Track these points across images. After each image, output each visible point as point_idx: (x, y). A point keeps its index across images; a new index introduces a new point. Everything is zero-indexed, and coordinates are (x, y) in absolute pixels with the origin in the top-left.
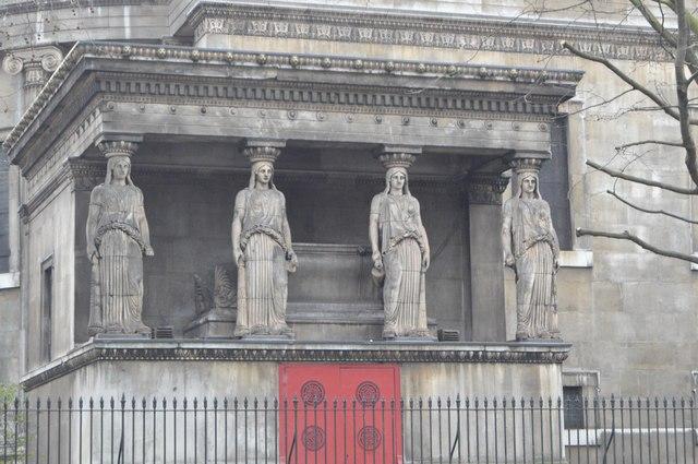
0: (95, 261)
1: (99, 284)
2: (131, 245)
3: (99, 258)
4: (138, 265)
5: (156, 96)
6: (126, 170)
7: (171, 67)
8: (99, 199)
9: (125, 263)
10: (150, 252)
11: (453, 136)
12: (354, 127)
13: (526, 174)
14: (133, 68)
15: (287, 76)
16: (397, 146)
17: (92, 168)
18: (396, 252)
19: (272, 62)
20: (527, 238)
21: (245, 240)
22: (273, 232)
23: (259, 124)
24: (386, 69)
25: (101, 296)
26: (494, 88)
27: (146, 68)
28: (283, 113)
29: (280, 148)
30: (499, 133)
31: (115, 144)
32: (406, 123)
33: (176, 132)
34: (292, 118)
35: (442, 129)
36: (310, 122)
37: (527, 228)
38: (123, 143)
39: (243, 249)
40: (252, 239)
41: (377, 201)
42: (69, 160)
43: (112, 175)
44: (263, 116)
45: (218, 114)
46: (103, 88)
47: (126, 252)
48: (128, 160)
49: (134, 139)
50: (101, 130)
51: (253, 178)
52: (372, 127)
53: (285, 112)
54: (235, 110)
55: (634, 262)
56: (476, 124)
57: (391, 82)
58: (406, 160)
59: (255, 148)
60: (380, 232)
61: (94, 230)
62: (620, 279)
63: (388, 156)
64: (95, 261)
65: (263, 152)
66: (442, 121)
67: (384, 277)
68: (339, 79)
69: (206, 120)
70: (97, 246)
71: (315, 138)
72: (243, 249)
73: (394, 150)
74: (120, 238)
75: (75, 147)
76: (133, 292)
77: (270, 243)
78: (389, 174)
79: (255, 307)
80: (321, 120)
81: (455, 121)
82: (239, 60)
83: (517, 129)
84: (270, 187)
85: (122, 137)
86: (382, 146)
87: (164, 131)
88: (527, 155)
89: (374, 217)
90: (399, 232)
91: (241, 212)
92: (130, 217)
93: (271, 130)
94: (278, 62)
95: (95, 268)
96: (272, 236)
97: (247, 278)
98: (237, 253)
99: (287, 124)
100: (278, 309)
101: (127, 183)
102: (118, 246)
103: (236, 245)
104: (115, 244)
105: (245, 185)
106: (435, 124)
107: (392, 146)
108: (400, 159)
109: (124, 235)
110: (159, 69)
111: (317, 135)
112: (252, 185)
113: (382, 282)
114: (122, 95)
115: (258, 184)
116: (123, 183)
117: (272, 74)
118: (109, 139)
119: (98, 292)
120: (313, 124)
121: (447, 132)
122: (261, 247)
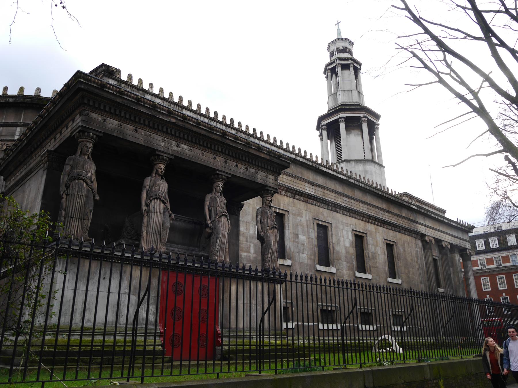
0: (64, 196)
1: (65, 210)
2: (88, 190)
3: (67, 195)
4: (92, 202)
5: (114, 115)
6: (90, 150)
7: (124, 101)
8: (71, 163)
9: (83, 200)
10: (98, 198)
11: (243, 173)
12: (204, 158)
13: (268, 197)
14: (105, 95)
15: (180, 123)
16: (222, 171)
17: (70, 146)
18: (219, 221)
19: (175, 114)
20: (269, 225)
21: (149, 201)
22: (164, 200)
23: (162, 144)
24: (223, 133)
25: (65, 218)
26: (262, 155)
27: (112, 97)
28: (174, 143)
29: (169, 159)
30: (261, 177)
31: (86, 134)
32: (226, 162)
33: (121, 137)
34: (178, 146)
35: (240, 169)
36: (185, 149)
37: (269, 220)
38: (91, 134)
39: (147, 205)
40: (153, 201)
41: (208, 197)
42: (48, 151)
43: (81, 152)
44: (164, 141)
45: (143, 133)
46: (86, 101)
47: (85, 193)
48: (92, 145)
49: (98, 134)
50: (80, 124)
51: (155, 172)
52: (212, 160)
53: (174, 142)
54: (152, 134)
55: (250, 256)
56: (253, 171)
57: (224, 140)
58: (224, 179)
59: (159, 155)
60: (210, 211)
61: (66, 178)
62: (245, 262)
63: (216, 176)
64: (64, 196)
65: (163, 159)
66: (240, 166)
67: (212, 233)
68: (203, 132)
69: (137, 135)
70: (67, 187)
71: (187, 158)
72: (147, 205)
73: (220, 173)
74: (82, 185)
75: (52, 145)
76: (86, 218)
77: (162, 205)
78: (215, 185)
79: (152, 237)
80: (190, 150)
81: (244, 167)
82: (160, 108)
83: (266, 176)
84: (162, 178)
85: (91, 131)
86: (216, 170)
87: (115, 134)
88: (270, 189)
89: (207, 204)
90: (221, 213)
91: (147, 187)
92: (89, 175)
93: (168, 149)
94: (177, 115)
95: (64, 200)
96: (163, 202)
97: (148, 222)
98: (144, 208)
99: (175, 148)
100: (163, 241)
101: (89, 158)
102: (81, 189)
103: (143, 203)
104: (79, 188)
105: (150, 175)
106: (237, 166)
107: (220, 171)
108: (222, 178)
109: (85, 185)
110: (119, 100)
111: (188, 157)
112: (154, 175)
113: (210, 235)
114: (95, 109)
115: (157, 175)
116: (86, 157)
117: (173, 120)
118: (83, 131)
119: (63, 215)
120: (187, 151)
121: (241, 170)
122: (158, 206)
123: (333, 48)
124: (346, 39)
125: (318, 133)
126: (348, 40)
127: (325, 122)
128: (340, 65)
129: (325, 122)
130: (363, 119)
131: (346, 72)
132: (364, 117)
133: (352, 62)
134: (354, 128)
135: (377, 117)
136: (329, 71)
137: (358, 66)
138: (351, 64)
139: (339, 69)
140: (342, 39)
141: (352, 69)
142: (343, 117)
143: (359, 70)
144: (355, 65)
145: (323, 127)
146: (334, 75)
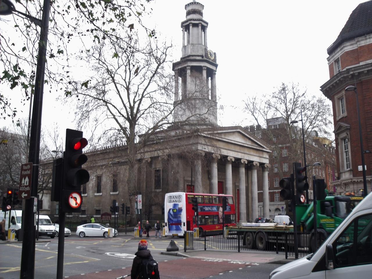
134: (197, 74)
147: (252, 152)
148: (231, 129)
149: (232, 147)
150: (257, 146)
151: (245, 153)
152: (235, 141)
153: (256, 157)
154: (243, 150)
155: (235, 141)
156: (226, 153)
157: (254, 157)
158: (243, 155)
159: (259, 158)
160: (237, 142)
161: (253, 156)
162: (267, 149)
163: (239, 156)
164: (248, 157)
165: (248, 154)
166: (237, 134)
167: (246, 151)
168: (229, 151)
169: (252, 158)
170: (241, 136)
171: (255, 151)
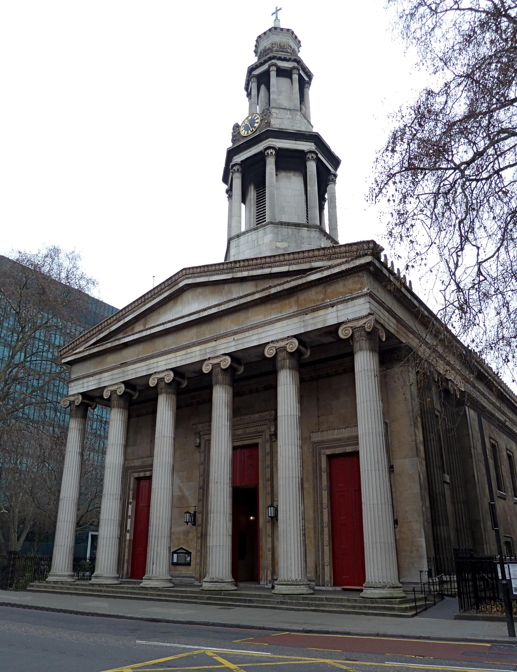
123: (265, 44)
124: (288, 30)
125: (226, 187)
126: (293, 33)
127: (238, 159)
128: (274, 68)
129: (238, 159)
130: (310, 156)
131: (284, 82)
132: (311, 152)
133: (295, 64)
135: (336, 162)
136: (254, 80)
137: (306, 79)
138: (294, 68)
139: (273, 74)
140: (282, 29)
141: (295, 77)
142: (273, 148)
143: (307, 85)
144: (301, 72)
145: (235, 168)
146: (263, 87)
147: (256, 316)
148: (154, 299)
149: (170, 341)
150: (286, 279)
151: (216, 339)
152: (163, 324)
153: (279, 324)
154: (207, 331)
155: (163, 324)
156: (145, 368)
157: (267, 328)
158: (213, 344)
159: (296, 320)
160: (170, 321)
161: (260, 330)
162: (330, 267)
163: (194, 355)
164: (233, 343)
165: (235, 333)
166: (188, 296)
167: (228, 324)
168: (152, 361)
169: (251, 340)
170: (207, 289)
171: (269, 307)
